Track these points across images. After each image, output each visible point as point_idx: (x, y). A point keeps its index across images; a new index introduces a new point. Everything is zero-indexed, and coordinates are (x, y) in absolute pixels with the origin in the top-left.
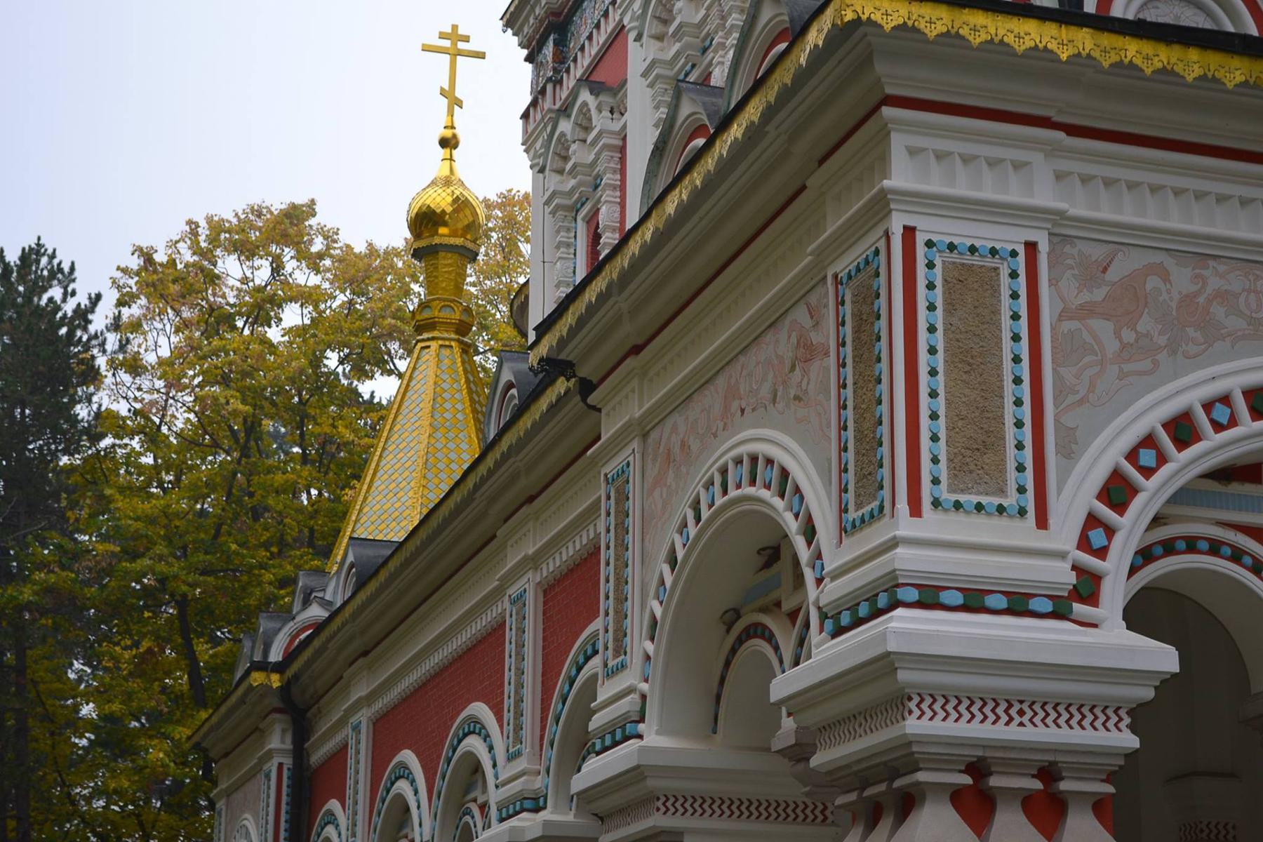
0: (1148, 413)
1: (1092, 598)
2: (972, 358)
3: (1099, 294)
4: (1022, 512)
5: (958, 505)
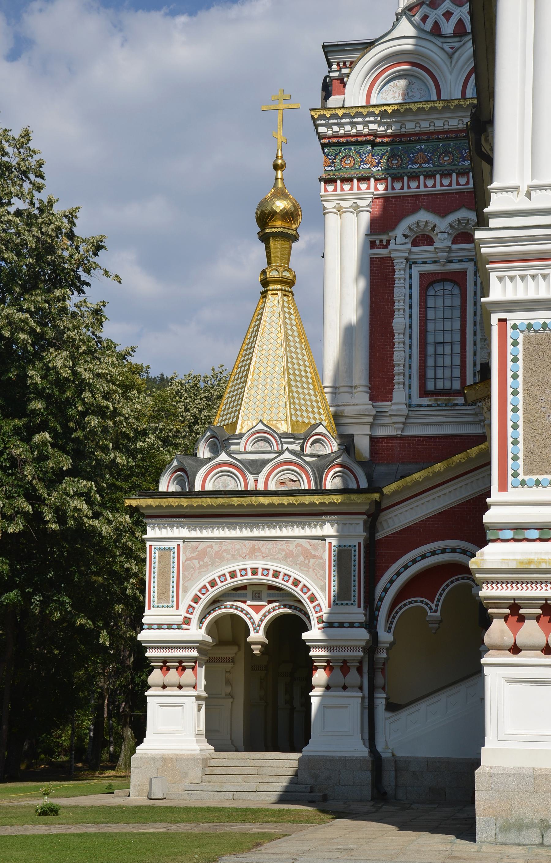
0: (205, 580)
1: (188, 623)
2: (164, 573)
3: (195, 554)
4: (172, 607)
5: (158, 607)
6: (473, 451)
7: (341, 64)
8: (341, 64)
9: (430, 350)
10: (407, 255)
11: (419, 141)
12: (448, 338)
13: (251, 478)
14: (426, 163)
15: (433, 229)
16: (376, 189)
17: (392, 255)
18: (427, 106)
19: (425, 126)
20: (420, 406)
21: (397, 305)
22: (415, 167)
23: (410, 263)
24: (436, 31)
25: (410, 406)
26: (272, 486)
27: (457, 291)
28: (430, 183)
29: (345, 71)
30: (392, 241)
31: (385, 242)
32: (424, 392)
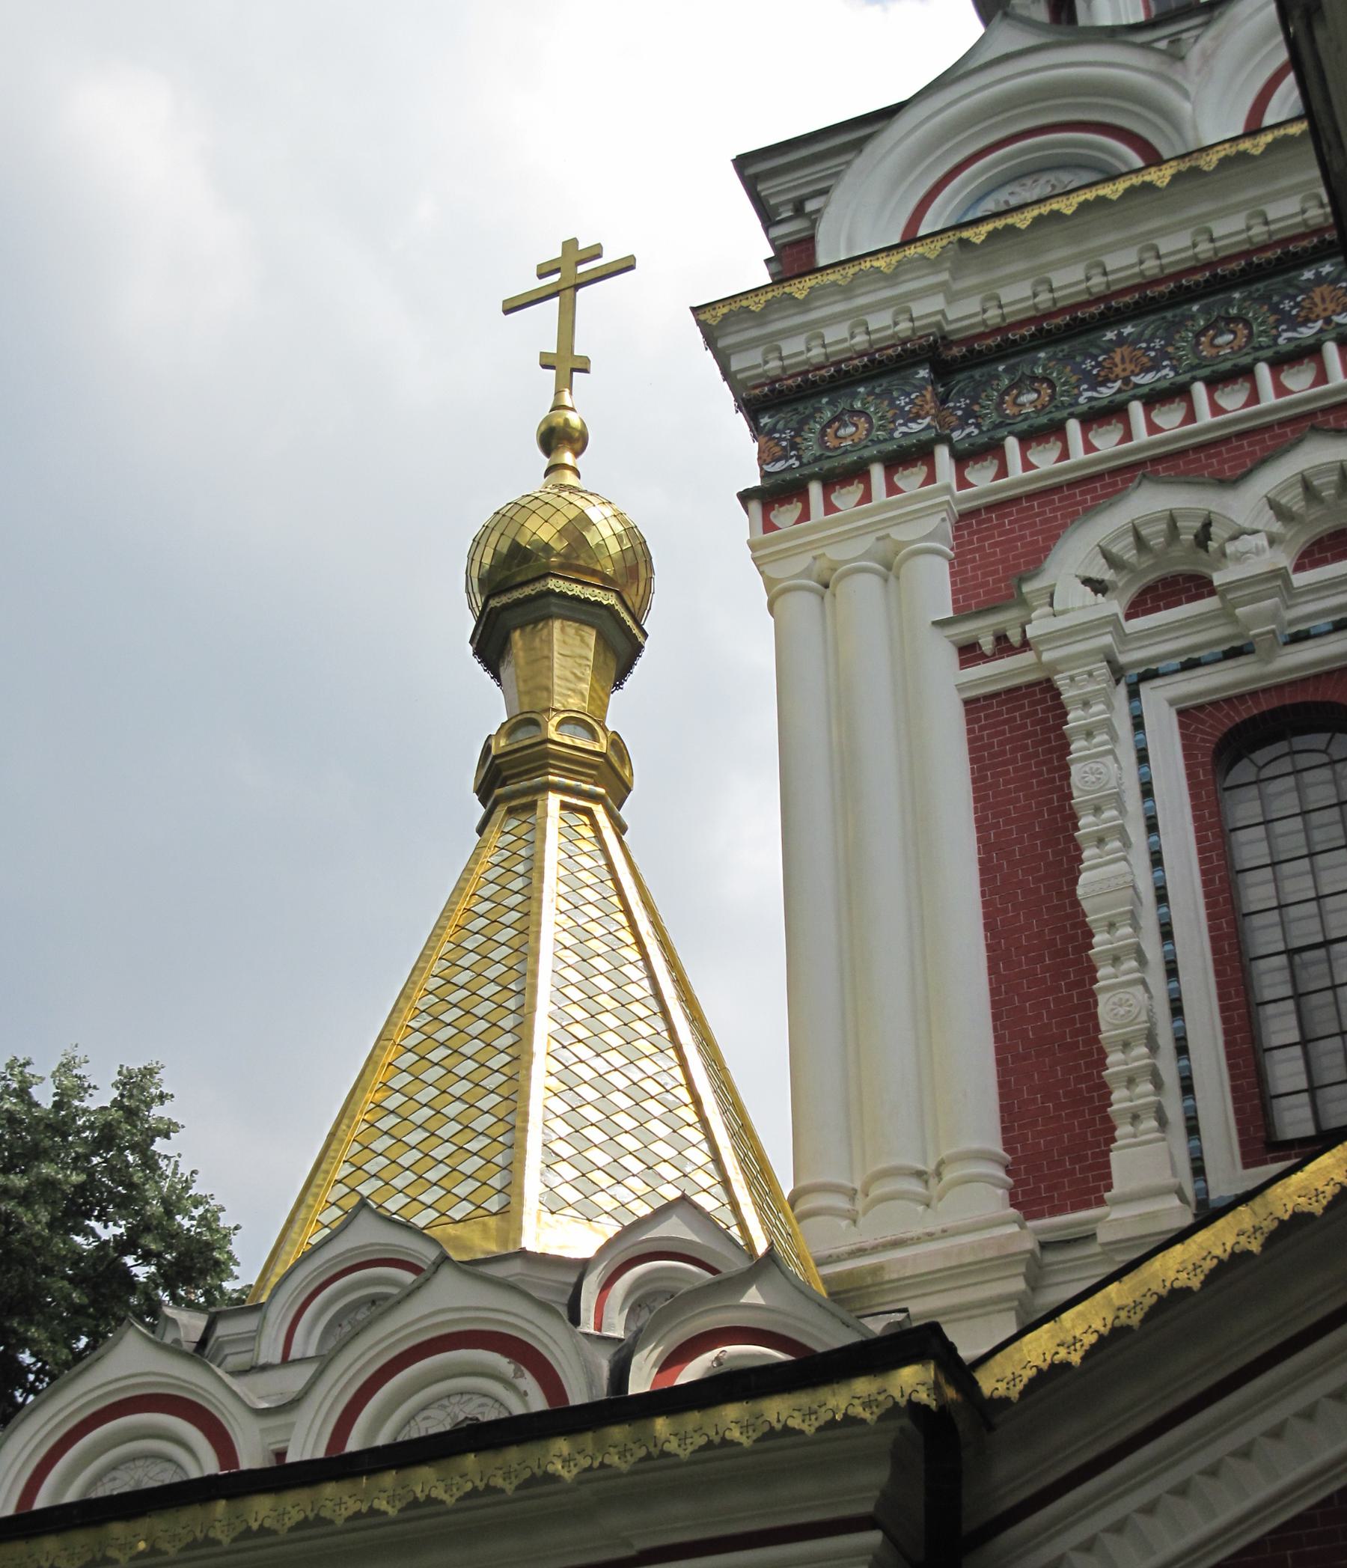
9: (1271, 980)
14: (1147, 370)
15: (1203, 537)
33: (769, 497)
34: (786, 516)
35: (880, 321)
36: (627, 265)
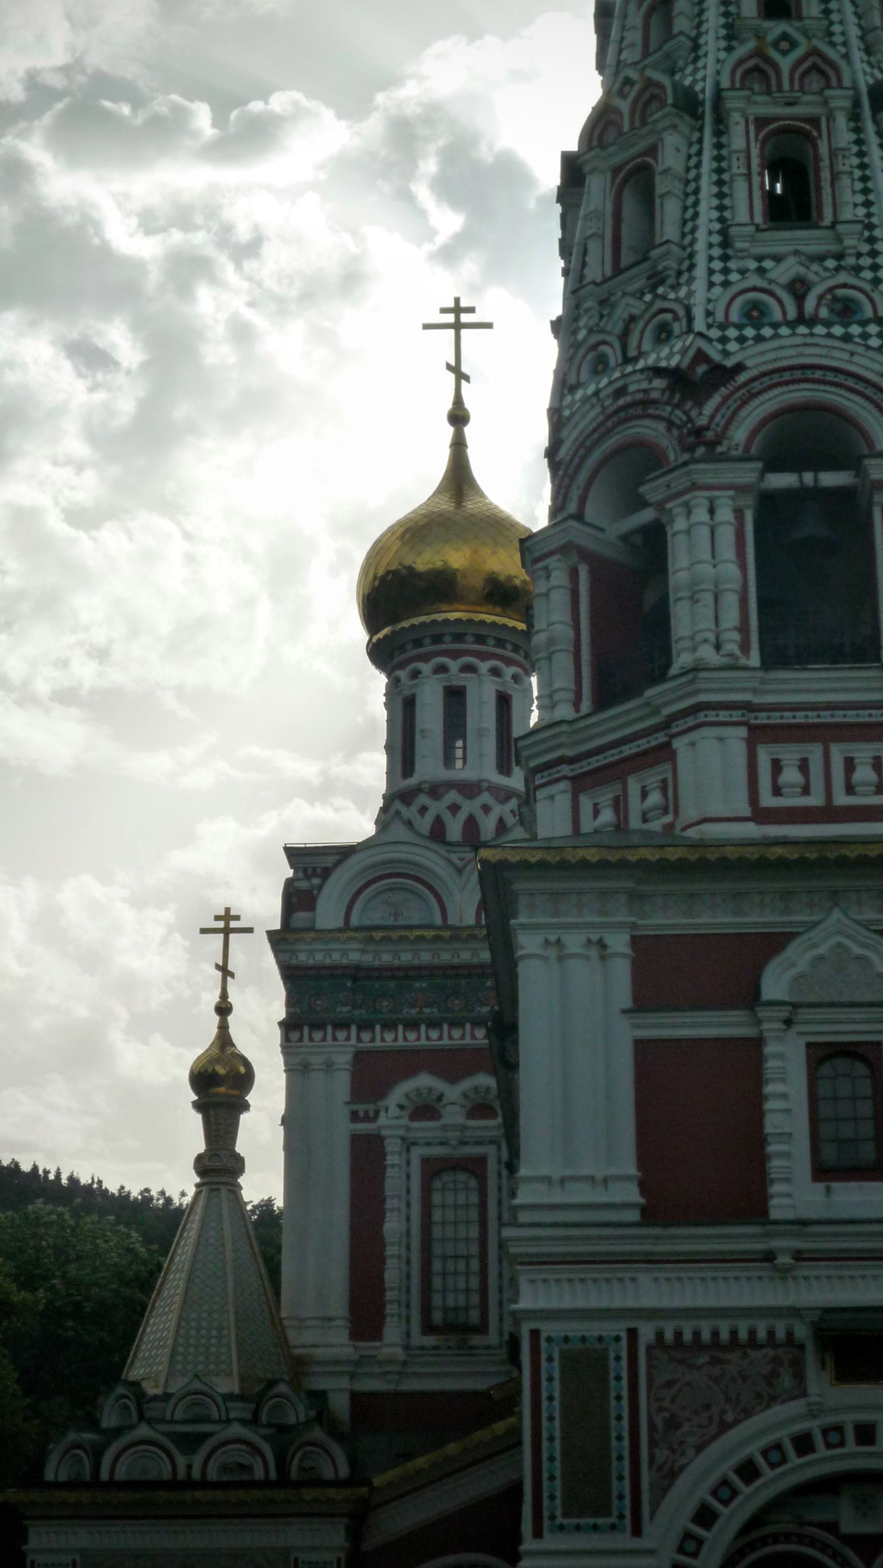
6: (500, 1427)
7: (310, 871)
8: (310, 871)
9: (437, 1266)
10: (401, 1132)
11: (419, 977)
12: (462, 1249)
13: (181, 1461)
16: (359, 1040)
17: (384, 1133)
18: (429, 934)
19: (426, 958)
20: (422, 1348)
21: (389, 1204)
22: (414, 1011)
23: (408, 1144)
24: (438, 833)
25: (407, 1348)
26: (213, 1474)
27: (473, 1183)
28: (434, 1034)
29: (316, 881)
30: (382, 1114)
31: (371, 1114)
32: (428, 1328)
33: (288, 1026)
34: (295, 1036)
35: (336, 956)
36: (250, 930)
